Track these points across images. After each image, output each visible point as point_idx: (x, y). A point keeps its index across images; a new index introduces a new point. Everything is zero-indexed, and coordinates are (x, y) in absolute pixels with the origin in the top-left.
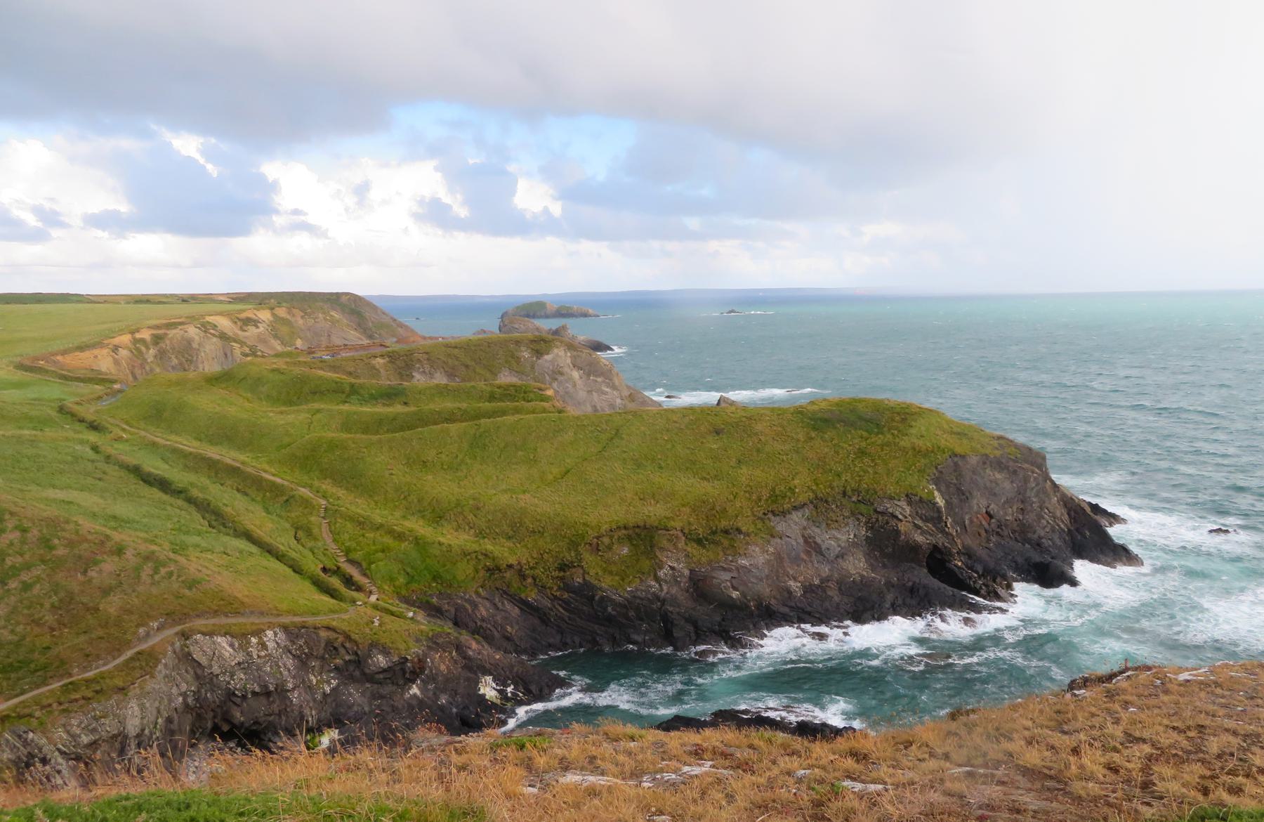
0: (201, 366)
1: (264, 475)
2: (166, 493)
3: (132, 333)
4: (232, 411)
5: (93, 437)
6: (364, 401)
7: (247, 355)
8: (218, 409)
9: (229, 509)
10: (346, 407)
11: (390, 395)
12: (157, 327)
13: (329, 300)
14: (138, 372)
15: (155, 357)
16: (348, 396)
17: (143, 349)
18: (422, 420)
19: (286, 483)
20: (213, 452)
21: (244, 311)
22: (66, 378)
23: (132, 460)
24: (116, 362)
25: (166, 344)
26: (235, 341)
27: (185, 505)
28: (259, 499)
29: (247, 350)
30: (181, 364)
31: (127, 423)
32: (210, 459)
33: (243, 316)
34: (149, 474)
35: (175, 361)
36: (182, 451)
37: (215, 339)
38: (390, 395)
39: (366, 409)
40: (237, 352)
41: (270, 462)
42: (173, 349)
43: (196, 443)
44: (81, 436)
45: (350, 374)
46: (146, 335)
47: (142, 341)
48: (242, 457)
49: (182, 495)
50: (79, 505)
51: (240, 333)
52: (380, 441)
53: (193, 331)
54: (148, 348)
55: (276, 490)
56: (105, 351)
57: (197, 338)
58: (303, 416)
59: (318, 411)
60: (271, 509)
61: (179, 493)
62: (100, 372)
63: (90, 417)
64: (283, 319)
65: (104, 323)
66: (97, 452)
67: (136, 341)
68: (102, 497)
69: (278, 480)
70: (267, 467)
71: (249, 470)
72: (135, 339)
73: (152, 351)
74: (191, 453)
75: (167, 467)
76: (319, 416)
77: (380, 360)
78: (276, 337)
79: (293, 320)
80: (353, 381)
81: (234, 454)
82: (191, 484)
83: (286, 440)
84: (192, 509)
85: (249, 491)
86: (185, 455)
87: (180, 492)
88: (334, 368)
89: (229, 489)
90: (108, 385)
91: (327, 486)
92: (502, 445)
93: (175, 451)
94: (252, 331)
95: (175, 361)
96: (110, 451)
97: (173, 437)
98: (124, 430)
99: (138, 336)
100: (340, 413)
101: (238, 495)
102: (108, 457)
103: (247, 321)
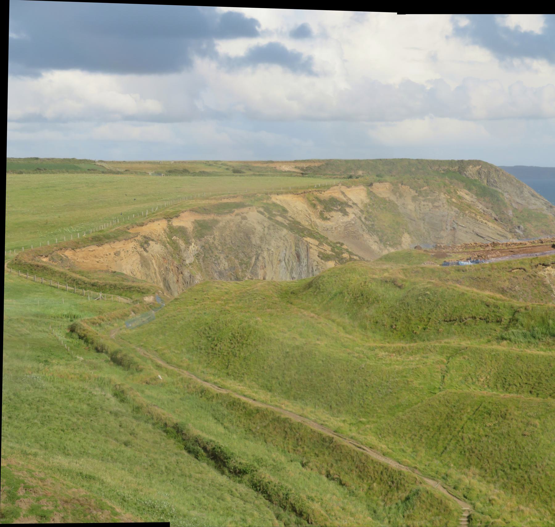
0: (261, 272)
1: (374, 456)
2: (223, 473)
3: (169, 218)
4: (323, 345)
5: (116, 376)
6: (532, 337)
7: (326, 258)
8: (300, 341)
9: (316, 506)
10: (503, 347)
12: (205, 210)
13: (447, 172)
14: (172, 278)
15: (197, 256)
16: (506, 329)
17: (182, 244)
19: (404, 469)
20: (290, 409)
21: (328, 187)
22: (80, 283)
23: (175, 419)
24: (145, 262)
25: (214, 238)
26: (311, 234)
27: (252, 493)
28: (362, 493)
29: (328, 250)
30: (233, 268)
31: (162, 356)
32: (285, 421)
33: (326, 195)
34: (197, 441)
35: (224, 264)
36: (244, 407)
37: (285, 231)
39: (538, 351)
40: (314, 253)
41: (380, 433)
43: (263, 395)
44: (101, 375)
45: (503, 291)
46: (186, 221)
47: (182, 231)
48: (335, 422)
49: (246, 477)
50: (102, 482)
51: (319, 221)
53: (254, 217)
55: (392, 481)
56: (131, 245)
57: (259, 228)
58: (433, 358)
59: (458, 351)
60: (380, 510)
61: (238, 473)
62: (124, 277)
63: (112, 346)
64: (384, 200)
66: (122, 401)
68: (130, 471)
69: (393, 465)
70: (372, 439)
71: (345, 443)
72: (170, 227)
73: (194, 248)
74: (258, 410)
75: (221, 429)
76: (458, 359)
78: (372, 230)
80: (516, 303)
81: (323, 415)
82: (259, 461)
83: (405, 397)
84: (261, 500)
85: (346, 479)
86: (250, 413)
87: (244, 472)
88: (478, 281)
89: (314, 473)
90: (136, 296)
91: (471, 480)
93: (233, 404)
94: (337, 219)
95: (224, 264)
96: (141, 399)
97: (231, 383)
98: (159, 367)
99: (176, 223)
100: (495, 356)
101: (332, 486)
102: (137, 409)
103: (332, 205)
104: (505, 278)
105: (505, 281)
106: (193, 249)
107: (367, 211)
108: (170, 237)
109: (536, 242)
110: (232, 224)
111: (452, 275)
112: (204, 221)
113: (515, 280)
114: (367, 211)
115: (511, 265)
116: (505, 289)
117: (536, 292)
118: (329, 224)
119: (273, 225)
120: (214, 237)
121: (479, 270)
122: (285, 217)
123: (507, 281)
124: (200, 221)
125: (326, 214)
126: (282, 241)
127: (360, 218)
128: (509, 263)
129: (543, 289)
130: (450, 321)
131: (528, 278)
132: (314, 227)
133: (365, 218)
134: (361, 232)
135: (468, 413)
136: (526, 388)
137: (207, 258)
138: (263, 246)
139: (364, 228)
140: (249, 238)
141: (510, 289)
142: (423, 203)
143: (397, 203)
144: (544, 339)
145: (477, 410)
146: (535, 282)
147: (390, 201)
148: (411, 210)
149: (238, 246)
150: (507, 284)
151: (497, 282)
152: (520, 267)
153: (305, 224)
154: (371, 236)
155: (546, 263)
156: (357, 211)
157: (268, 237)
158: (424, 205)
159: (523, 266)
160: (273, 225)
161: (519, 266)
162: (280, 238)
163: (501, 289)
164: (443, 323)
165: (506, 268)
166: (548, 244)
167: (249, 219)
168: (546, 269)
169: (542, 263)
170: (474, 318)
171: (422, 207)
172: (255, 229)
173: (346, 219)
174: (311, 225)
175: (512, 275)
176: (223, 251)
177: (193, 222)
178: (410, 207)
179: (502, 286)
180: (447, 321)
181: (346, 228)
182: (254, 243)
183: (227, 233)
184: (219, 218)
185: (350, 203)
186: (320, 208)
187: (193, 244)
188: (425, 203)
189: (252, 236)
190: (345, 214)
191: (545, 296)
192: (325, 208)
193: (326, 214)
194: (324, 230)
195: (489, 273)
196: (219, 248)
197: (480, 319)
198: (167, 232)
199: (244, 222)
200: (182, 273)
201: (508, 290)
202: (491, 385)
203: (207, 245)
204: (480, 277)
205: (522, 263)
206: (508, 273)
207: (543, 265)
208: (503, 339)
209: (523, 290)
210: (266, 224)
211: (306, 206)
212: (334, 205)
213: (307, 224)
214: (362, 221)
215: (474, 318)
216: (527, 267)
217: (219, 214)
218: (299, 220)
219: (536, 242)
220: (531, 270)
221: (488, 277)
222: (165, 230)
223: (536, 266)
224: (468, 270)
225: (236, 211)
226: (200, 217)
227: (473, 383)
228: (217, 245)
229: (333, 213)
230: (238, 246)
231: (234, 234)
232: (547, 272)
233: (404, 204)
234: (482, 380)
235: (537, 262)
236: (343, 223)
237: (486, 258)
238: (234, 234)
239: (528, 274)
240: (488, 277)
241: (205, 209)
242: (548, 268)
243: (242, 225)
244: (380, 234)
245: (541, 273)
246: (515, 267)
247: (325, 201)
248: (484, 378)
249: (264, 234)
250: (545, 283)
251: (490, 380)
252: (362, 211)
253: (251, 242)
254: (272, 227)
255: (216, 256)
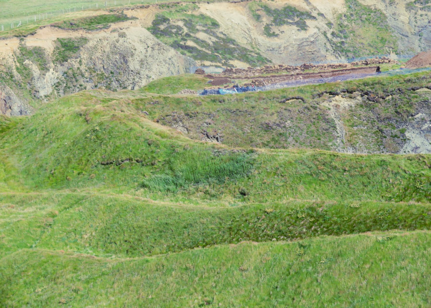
3: (21, 36)
11: (225, 174)
12: (72, 26)
15: (57, 86)
17: (35, 70)
18: (236, 230)
25: (80, 62)
26: (244, 55)
37: (172, 52)
38: (225, 174)
42: (92, 70)
46: (46, 41)
47: (38, 53)
52: (117, 271)
54: (44, 68)
57: (140, 48)
59: (79, 201)
65: (21, 15)
67: (25, 53)
73: (53, 75)
77: (343, 102)
78: (339, 49)
79: (388, 12)
92: (326, 297)
99: (31, 42)
104: (273, 111)
105: (273, 114)
106: (52, 76)
107: (340, 25)
108: (21, 61)
109: (360, 64)
110: (105, 43)
111: (203, 106)
112: (70, 39)
113: (287, 114)
114: (340, 25)
115: (285, 94)
116: (271, 124)
117: (313, 128)
118: (274, 42)
119: (159, 44)
120: (80, 61)
121: (241, 100)
122: (214, 34)
123: (275, 115)
124: (64, 39)
125: (275, 29)
126: (167, 65)
127: (325, 34)
128: (284, 91)
129: (324, 125)
130: (107, 164)
131: (306, 110)
132: (254, 46)
133: (333, 34)
134: (323, 52)
135: (28, 276)
136: (126, 246)
137: (69, 88)
138: (142, 72)
139: (329, 46)
140: (126, 62)
141: (278, 125)
142: (420, 12)
143: (385, 12)
144: (186, 186)
145: (23, 271)
146: (314, 116)
147: (376, 11)
148: (403, 22)
149: (111, 73)
150: (275, 118)
151: (261, 116)
152: (297, 96)
153: (243, 42)
154: (337, 57)
155: (334, 90)
156: (321, 23)
157: (150, 60)
158: (421, 15)
159: (302, 95)
160: (159, 44)
161: (297, 95)
162: (165, 61)
163: (265, 125)
164: (99, 166)
165: (278, 98)
166: (373, 65)
167: (128, 37)
168: (334, 99)
169: (328, 91)
170: (130, 159)
171: (419, 17)
172: (135, 50)
173: (303, 35)
174: (251, 43)
175: (284, 107)
176: (90, 79)
177: (54, 41)
178: (402, 18)
179: (267, 121)
180: (104, 164)
181: (300, 47)
182: (132, 68)
183: (98, 55)
184: (89, 36)
185: (314, 14)
186: (266, 20)
187: (51, 70)
188: (423, 13)
189: (130, 59)
190: (303, 27)
191: (324, 134)
192: (275, 21)
193: (275, 29)
194: (268, 50)
195: (254, 104)
196: (87, 75)
197: (137, 161)
198: (18, 54)
199: (121, 40)
200: (10, 108)
201: (274, 127)
202: (94, 242)
203: (70, 72)
204: (241, 109)
205: (301, 91)
206: (278, 104)
207: (331, 93)
208: (143, 186)
209: (296, 127)
210: (150, 43)
211: (245, 18)
212: (288, 17)
213: (245, 42)
214: (327, 37)
215: (130, 159)
216: (307, 97)
217: (89, 30)
218: (233, 37)
219: (360, 64)
220: (311, 100)
221: (250, 110)
222: (14, 52)
223: (320, 95)
224: (226, 101)
225: (113, 26)
226: (64, 35)
227: (75, 242)
228: (83, 71)
229: (285, 28)
230: (111, 73)
231: (108, 57)
232: (334, 103)
233: (394, 14)
234: (86, 237)
235: (323, 90)
236: (296, 40)
237: (261, 84)
238: (108, 57)
239: (305, 105)
240: (250, 110)
241: (71, 24)
242: (337, 97)
243: (118, 45)
244: (351, 55)
245: (326, 104)
246: (291, 96)
247: (276, 11)
248: (89, 235)
249: (146, 56)
250: (326, 117)
251: (94, 236)
252: (330, 24)
253: (128, 67)
254: (157, 47)
255: (81, 86)
